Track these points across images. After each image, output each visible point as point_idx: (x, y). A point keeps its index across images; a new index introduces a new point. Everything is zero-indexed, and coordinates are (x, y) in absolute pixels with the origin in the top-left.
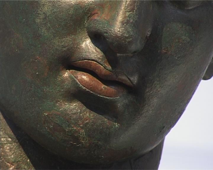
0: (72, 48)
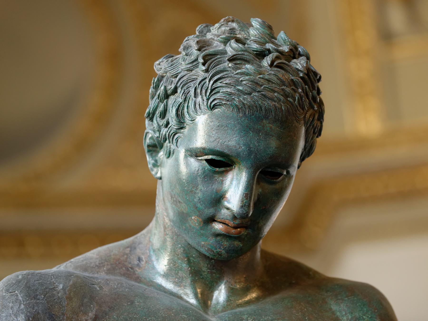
0: (215, 213)
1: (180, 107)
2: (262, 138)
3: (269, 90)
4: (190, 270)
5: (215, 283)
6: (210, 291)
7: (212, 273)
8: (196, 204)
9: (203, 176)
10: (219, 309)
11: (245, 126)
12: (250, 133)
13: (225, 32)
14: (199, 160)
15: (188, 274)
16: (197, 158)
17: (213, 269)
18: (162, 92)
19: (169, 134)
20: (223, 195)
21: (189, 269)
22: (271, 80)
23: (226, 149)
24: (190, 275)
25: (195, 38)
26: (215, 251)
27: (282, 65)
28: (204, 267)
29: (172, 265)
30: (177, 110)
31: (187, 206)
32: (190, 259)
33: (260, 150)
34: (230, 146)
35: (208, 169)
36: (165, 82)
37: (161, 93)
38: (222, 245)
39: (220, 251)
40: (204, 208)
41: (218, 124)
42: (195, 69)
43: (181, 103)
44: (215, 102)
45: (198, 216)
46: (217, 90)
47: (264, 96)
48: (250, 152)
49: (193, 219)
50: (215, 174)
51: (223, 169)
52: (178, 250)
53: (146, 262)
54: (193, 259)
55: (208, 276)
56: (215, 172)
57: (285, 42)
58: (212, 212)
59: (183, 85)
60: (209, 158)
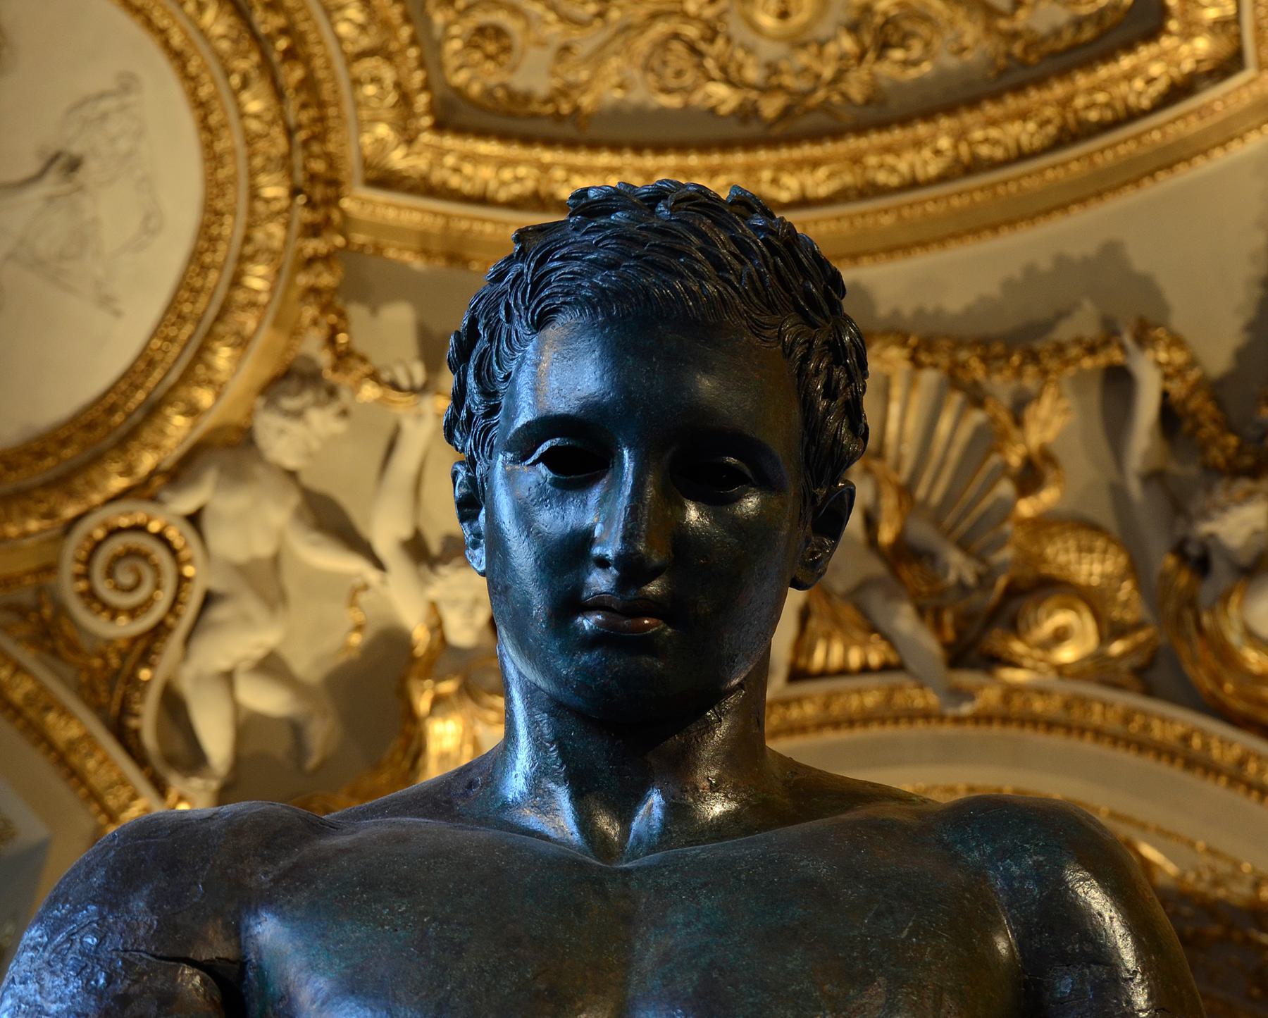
12: (628, 360)
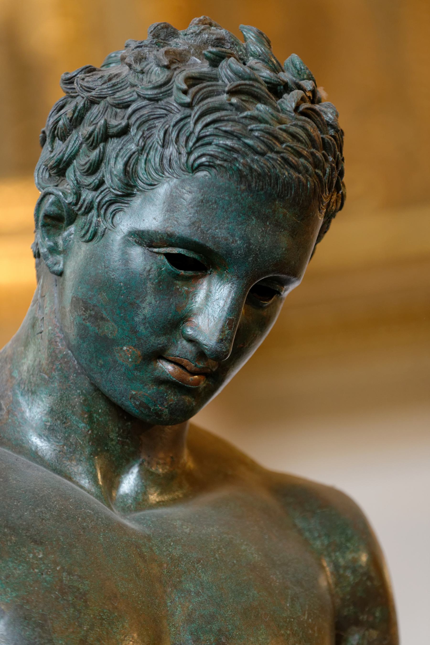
0: (166, 346)
1: (131, 159)
2: (270, 230)
3: (292, 151)
4: (90, 434)
5: (124, 461)
6: (116, 474)
7: (123, 444)
8: (137, 325)
9: (157, 281)
10: (130, 506)
11: (247, 206)
12: (253, 220)
13: (207, 42)
14: (154, 252)
15: (88, 440)
16: (150, 249)
17: (127, 438)
18: (100, 129)
19: (99, 202)
20: (186, 317)
21: (90, 432)
22: (297, 135)
23: (210, 241)
24: (89, 442)
25: (153, 44)
26: (152, 408)
27: (310, 112)
28: (112, 431)
29: (59, 422)
30: (126, 164)
31: (116, 327)
32: (93, 416)
33: (264, 250)
34: (217, 237)
35: (166, 270)
36: (101, 112)
37: (97, 130)
38: (166, 400)
39: (160, 409)
40: (149, 335)
41: (202, 198)
42: (165, 98)
43: (134, 153)
44: (204, 159)
45: (135, 346)
46: (206, 140)
47: (286, 160)
48: (249, 251)
49: (124, 351)
50: (177, 280)
51: (189, 273)
52: (75, 398)
53: (8, 412)
54: (97, 417)
55: (117, 448)
56: (178, 277)
57: (300, 73)
58: (162, 342)
59: (141, 123)
60: (174, 252)
